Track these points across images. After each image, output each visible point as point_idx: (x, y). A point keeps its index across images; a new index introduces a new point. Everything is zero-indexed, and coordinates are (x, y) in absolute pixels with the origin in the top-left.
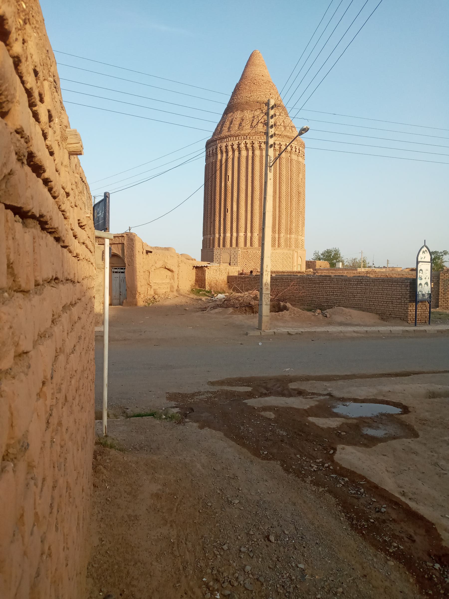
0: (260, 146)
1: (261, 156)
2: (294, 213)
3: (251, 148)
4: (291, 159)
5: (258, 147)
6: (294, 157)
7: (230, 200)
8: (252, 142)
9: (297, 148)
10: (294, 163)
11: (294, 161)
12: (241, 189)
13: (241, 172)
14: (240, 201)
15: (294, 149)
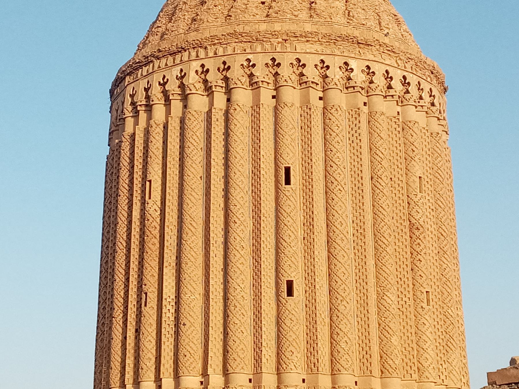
0: (251, 76)
1: (256, 105)
2: (391, 298)
3: (220, 83)
4: (370, 114)
5: (245, 80)
6: (381, 105)
7: (155, 264)
8: (224, 63)
9: (397, 75)
10: (383, 125)
11: (381, 119)
12: (187, 218)
13: (188, 162)
14: (184, 260)
15: (380, 81)
